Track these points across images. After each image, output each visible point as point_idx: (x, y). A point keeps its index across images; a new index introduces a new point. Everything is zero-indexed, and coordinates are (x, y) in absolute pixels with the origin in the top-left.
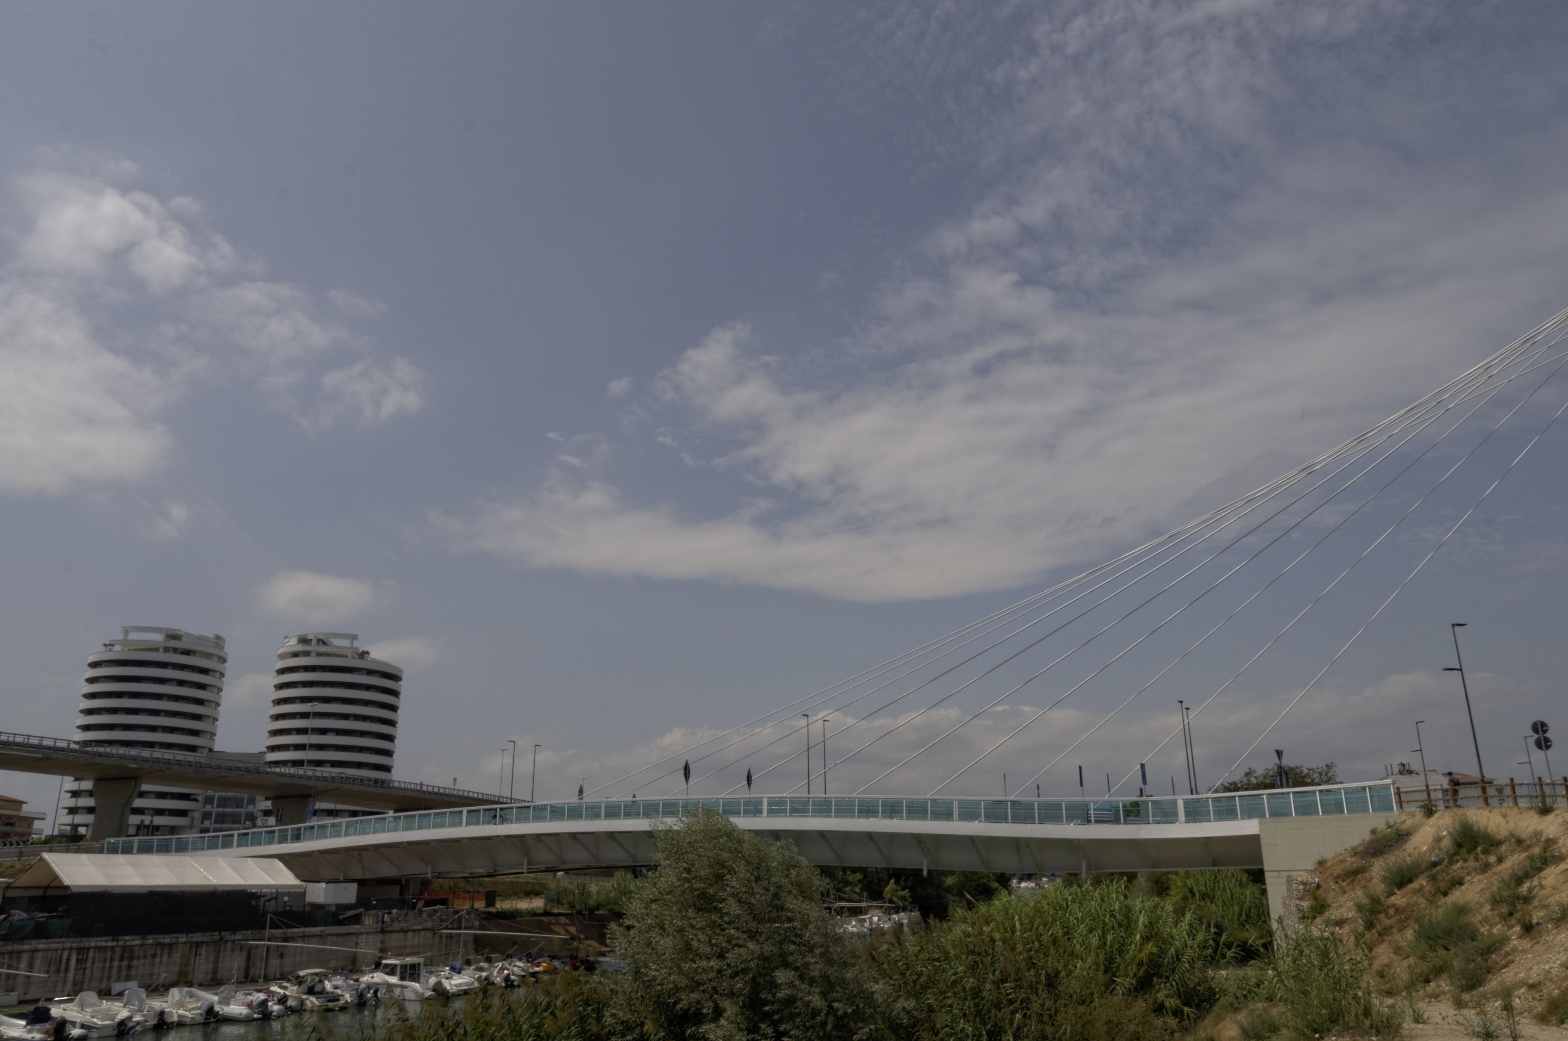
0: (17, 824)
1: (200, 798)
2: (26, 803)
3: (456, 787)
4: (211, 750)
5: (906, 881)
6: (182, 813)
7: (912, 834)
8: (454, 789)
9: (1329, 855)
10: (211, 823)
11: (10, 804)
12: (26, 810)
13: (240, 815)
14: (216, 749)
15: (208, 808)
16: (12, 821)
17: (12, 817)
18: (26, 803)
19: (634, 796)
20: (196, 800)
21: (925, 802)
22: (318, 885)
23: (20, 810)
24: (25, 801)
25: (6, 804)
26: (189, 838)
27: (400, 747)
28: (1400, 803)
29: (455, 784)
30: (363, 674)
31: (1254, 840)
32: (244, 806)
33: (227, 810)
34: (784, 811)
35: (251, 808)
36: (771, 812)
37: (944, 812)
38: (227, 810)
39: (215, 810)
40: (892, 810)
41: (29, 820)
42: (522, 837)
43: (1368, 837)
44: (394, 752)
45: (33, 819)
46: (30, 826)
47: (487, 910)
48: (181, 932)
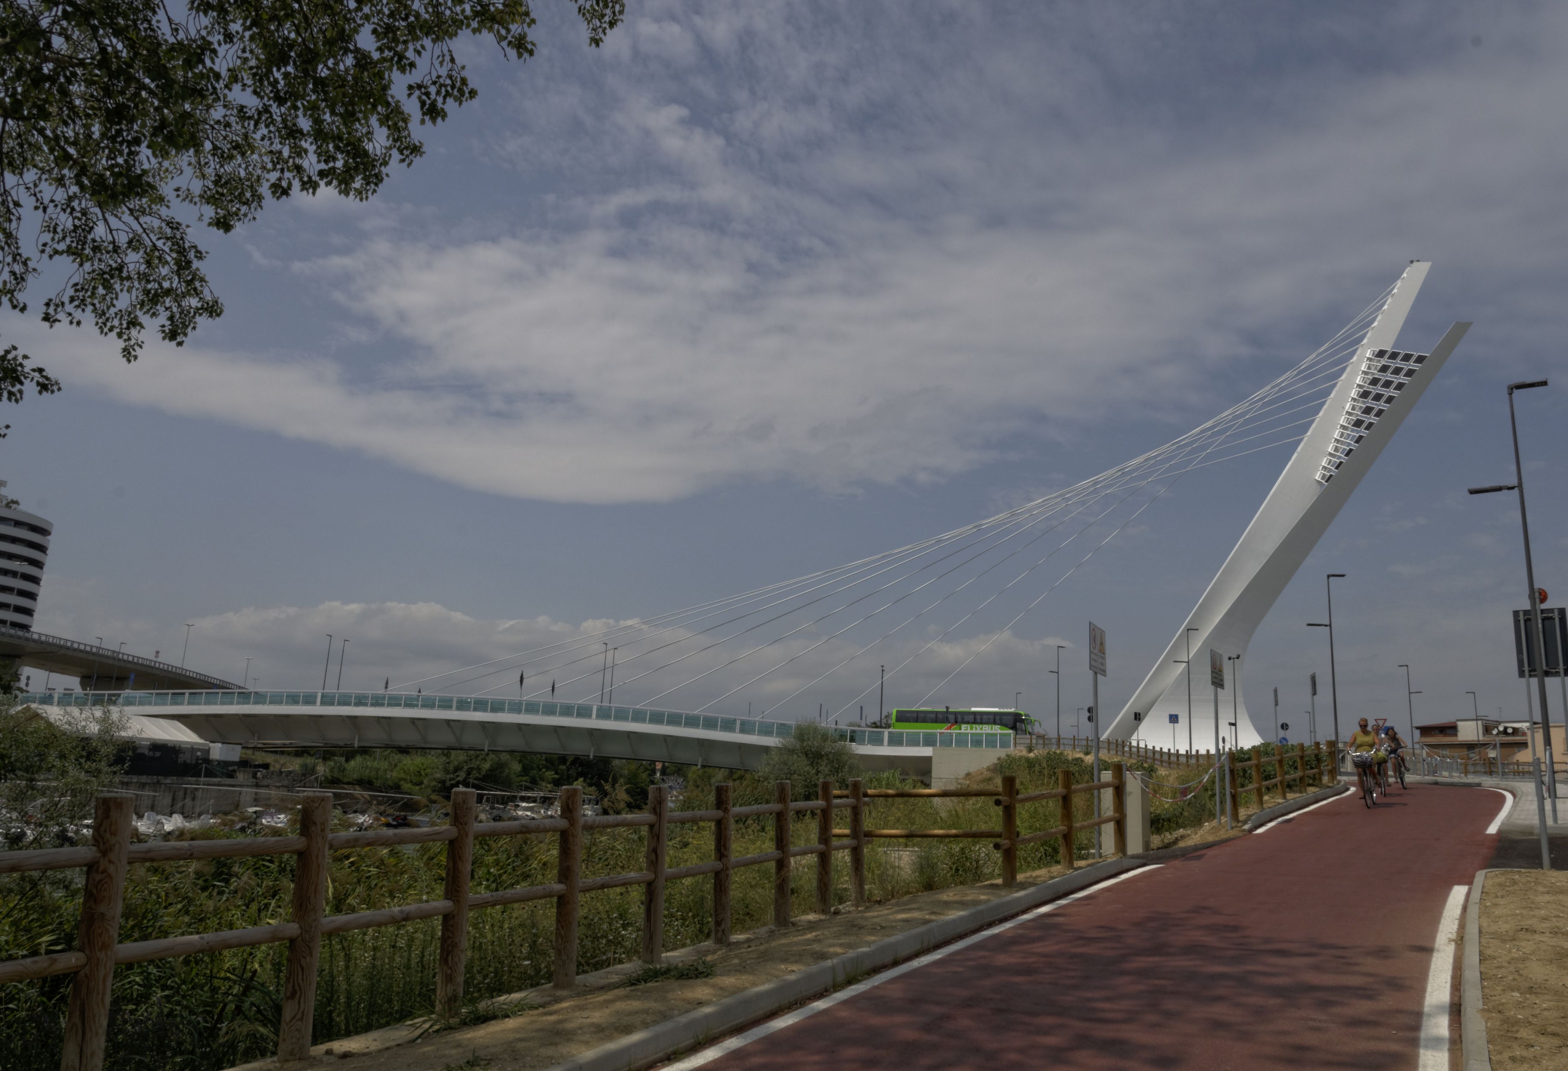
3: (158, 660)
5: (592, 778)
7: (698, 739)
8: (155, 662)
9: (972, 770)
19: (420, 692)
21: (755, 722)
22: (217, 744)
26: (902, 734)
27: (40, 606)
28: (1015, 744)
29: (157, 656)
30: (10, 525)
31: (928, 760)
34: (417, 706)
36: (598, 716)
37: (728, 725)
40: (692, 722)
42: (355, 717)
43: (996, 761)
44: (34, 611)
47: (568, 763)
48: (134, 774)
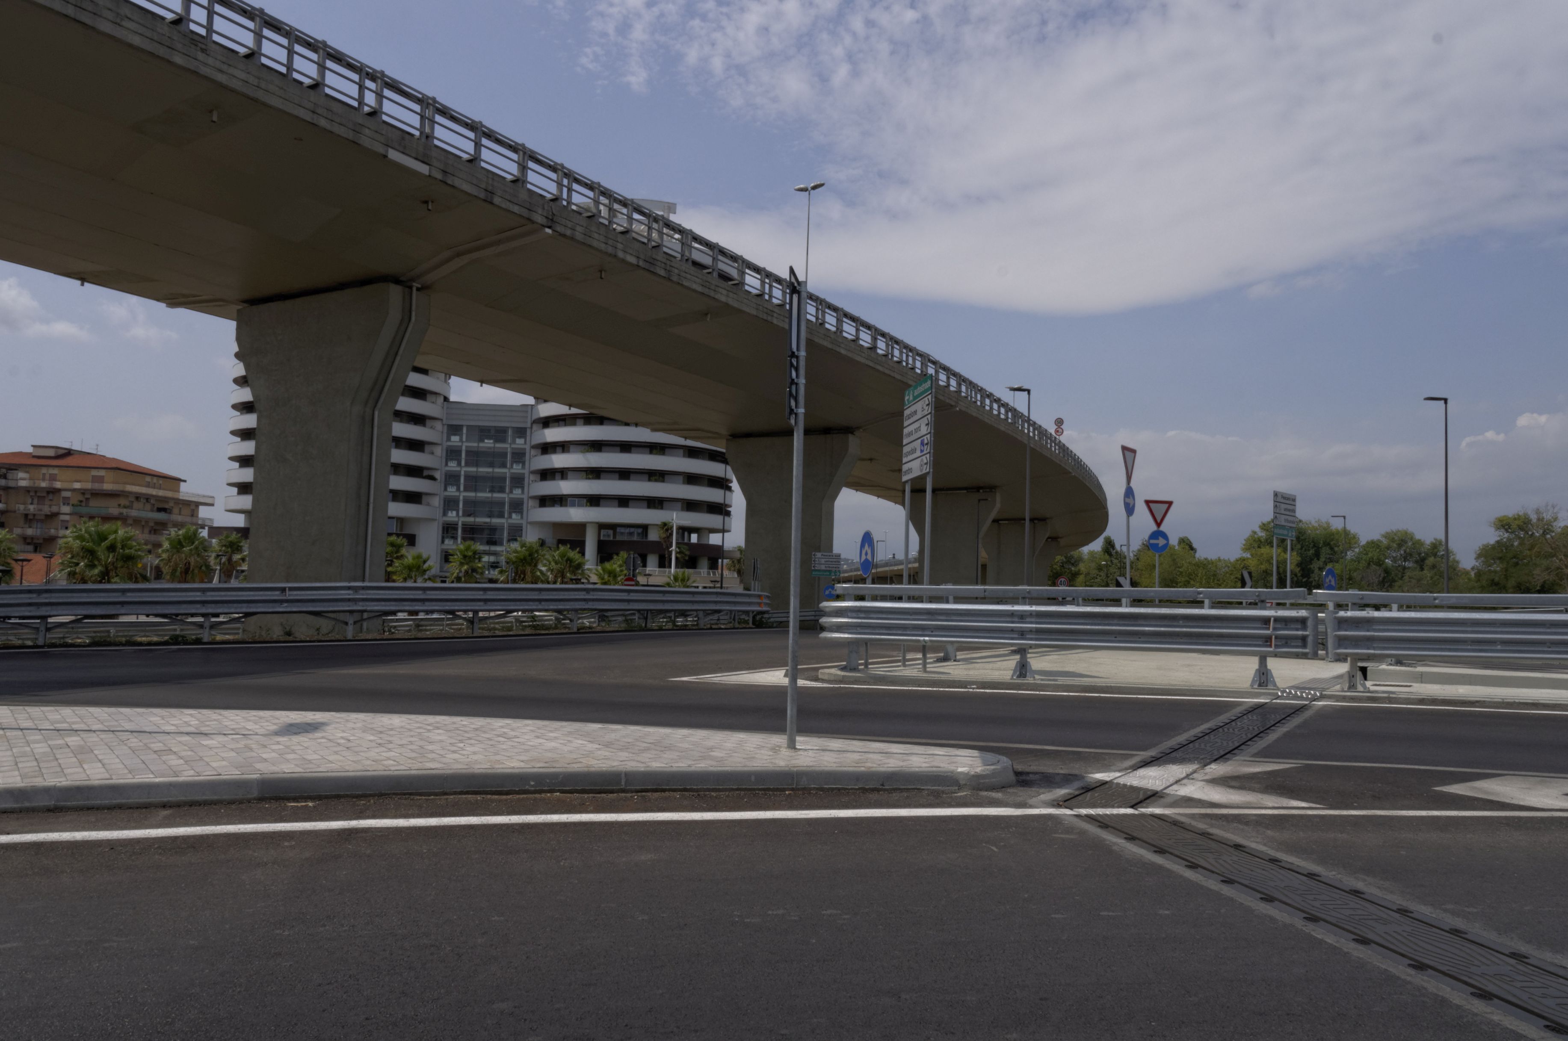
0: (176, 511)
1: (437, 475)
2: (185, 481)
4: (446, 399)
6: (413, 497)
10: (458, 514)
11: (161, 482)
12: (187, 491)
13: (502, 504)
14: (453, 398)
15: (452, 491)
16: (166, 506)
17: (165, 500)
18: (185, 481)
20: (432, 478)
23: (178, 491)
24: (183, 478)
25: (155, 480)
32: (507, 490)
33: (482, 495)
35: (517, 493)
38: (482, 495)
39: (463, 495)
41: (192, 506)
45: (198, 504)
46: (194, 513)
